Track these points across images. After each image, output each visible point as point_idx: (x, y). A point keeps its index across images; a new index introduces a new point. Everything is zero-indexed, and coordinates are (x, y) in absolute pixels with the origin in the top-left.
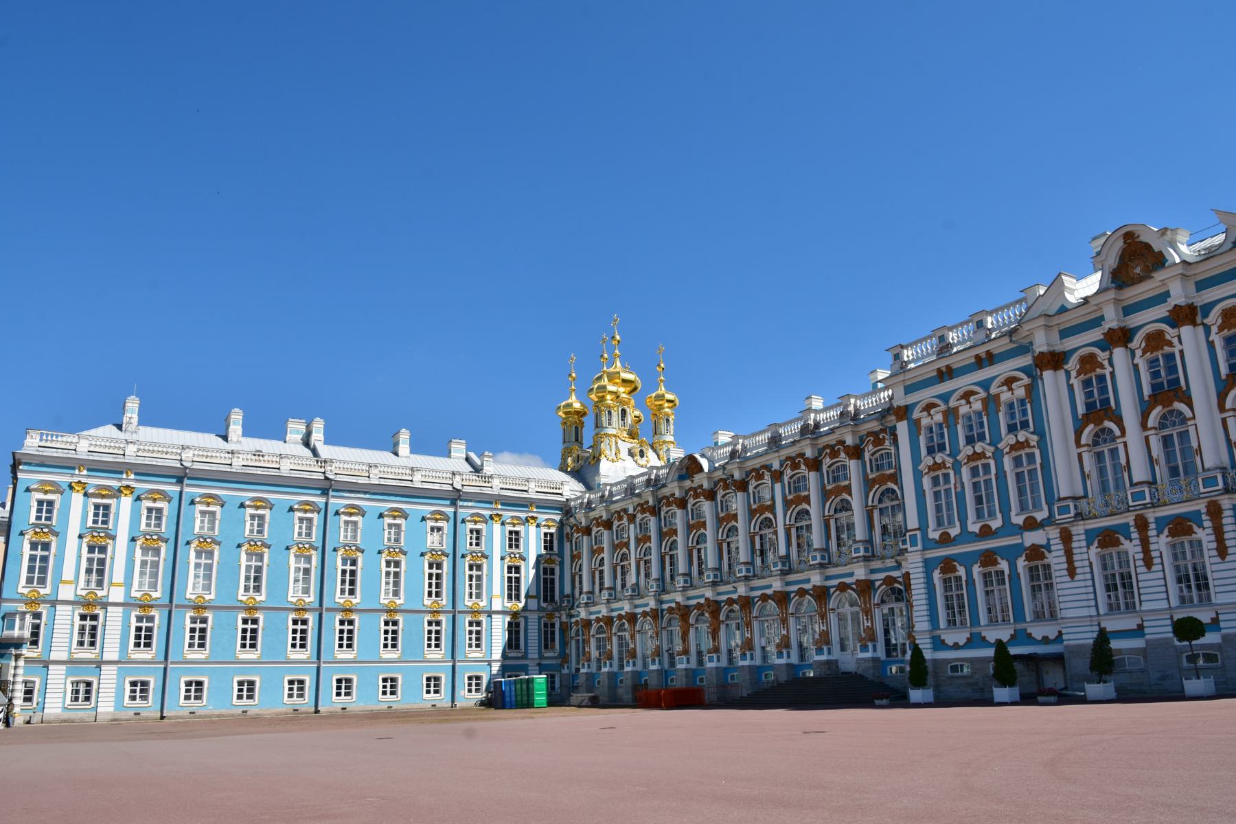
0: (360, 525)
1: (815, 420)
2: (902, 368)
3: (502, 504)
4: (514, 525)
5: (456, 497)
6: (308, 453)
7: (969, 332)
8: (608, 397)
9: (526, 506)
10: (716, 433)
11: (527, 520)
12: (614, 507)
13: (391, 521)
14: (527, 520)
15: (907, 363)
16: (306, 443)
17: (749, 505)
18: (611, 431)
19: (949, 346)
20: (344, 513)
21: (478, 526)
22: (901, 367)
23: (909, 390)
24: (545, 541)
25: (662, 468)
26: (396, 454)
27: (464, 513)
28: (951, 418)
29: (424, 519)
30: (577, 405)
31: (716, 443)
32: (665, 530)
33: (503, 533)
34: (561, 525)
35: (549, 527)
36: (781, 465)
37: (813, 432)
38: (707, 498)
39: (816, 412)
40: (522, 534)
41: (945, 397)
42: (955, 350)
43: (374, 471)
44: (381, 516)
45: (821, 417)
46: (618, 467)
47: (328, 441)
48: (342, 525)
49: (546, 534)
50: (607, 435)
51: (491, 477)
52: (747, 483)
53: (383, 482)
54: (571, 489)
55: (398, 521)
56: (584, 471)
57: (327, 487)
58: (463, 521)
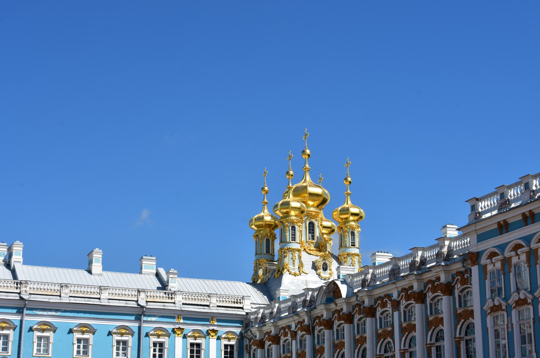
0: (51, 340)
1: (422, 257)
2: (476, 218)
3: (184, 319)
4: (195, 338)
5: (140, 313)
6: (8, 274)
7: (521, 191)
8: (293, 213)
9: (207, 320)
10: (374, 254)
11: (208, 333)
12: (282, 323)
13: (80, 336)
14: (208, 333)
15: (481, 214)
16: (8, 265)
17: (427, 318)
18: (295, 246)
19: (509, 202)
20: (37, 329)
21: (161, 340)
22: (476, 217)
23: (481, 238)
24: (226, 353)
25: (357, 275)
26: (90, 272)
27: (147, 327)
28: (506, 266)
29: (110, 333)
30: (268, 218)
31: (374, 264)
32: (317, 347)
33: (184, 345)
34: (241, 337)
35: (229, 339)
36: (399, 295)
37: (419, 268)
38: (417, 301)
39: (451, 239)
40: (203, 346)
41: (502, 247)
42: (513, 205)
43: (65, 291)
44: (71, 331)
45: (427, 254)
46: (299, 281)
47: (26, 262)
48: (36, 340)
49: (226, 346)
50: (289, 250)
51: (174, 293)
52: (375, 309)
53: (73, 300)
54: (253, 300)
55: (86, 336)
56: (268, 286)
57: (21, 306)
58: (147, 335)
